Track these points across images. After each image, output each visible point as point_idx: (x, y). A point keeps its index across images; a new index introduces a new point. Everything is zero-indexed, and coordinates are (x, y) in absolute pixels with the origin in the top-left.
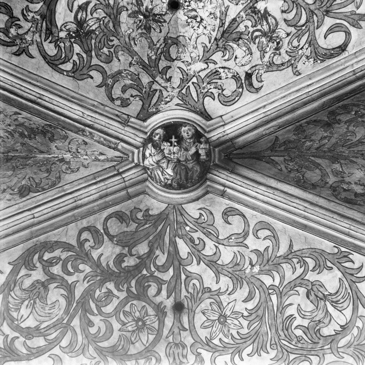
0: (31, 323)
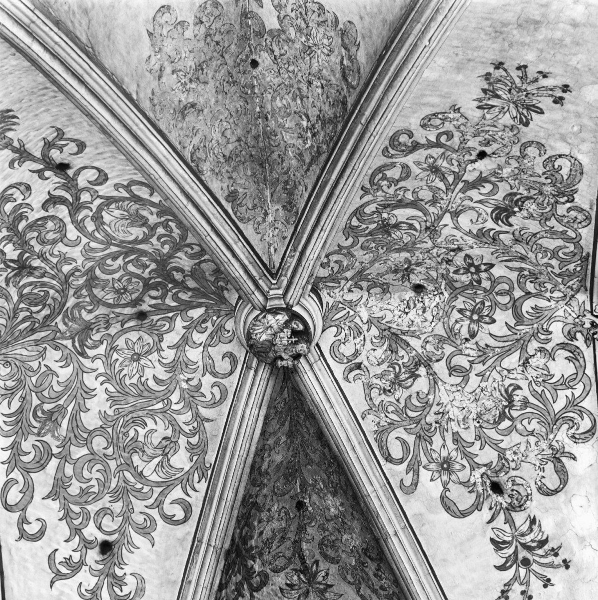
0: (107, 218)
